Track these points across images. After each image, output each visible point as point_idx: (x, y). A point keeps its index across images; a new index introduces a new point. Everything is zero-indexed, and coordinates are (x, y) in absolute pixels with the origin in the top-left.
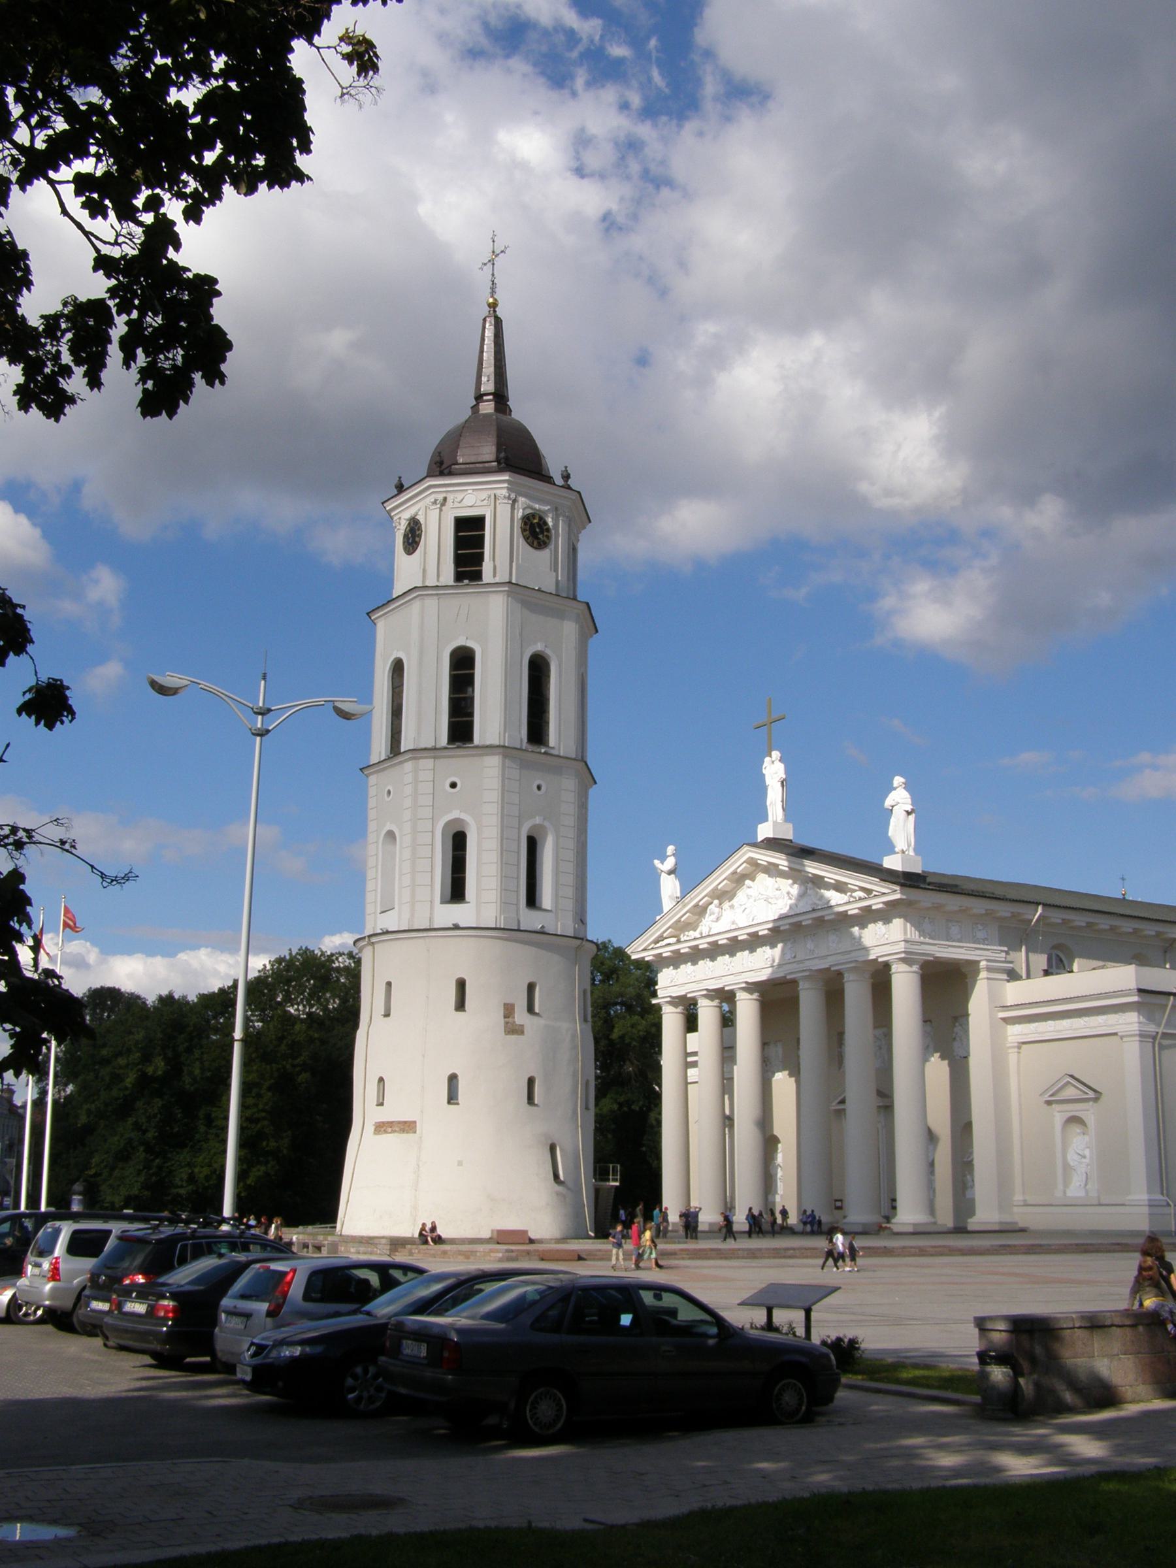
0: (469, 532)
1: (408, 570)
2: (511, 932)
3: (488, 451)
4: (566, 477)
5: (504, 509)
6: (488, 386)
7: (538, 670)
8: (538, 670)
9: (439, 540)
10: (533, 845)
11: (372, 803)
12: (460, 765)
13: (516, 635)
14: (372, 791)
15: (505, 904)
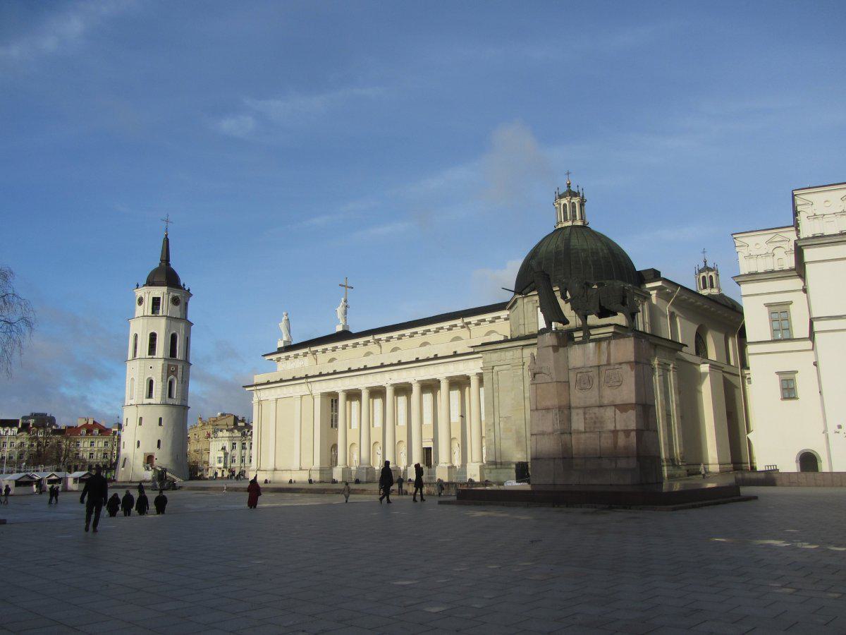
0: (156, 302)
1: (139, 310)
2: (166, 404)
3: (163, 279)
4: (184, 285)
5: (166, 296)
6: (165, 259)
7: (174, 338)
8: (174, 338)
9: (148, 303)
10: (171, 383)
11: (128, 370)
12: (151, 363)
13: (168, 328)
14: (128, 367)
15: (162, 398)
